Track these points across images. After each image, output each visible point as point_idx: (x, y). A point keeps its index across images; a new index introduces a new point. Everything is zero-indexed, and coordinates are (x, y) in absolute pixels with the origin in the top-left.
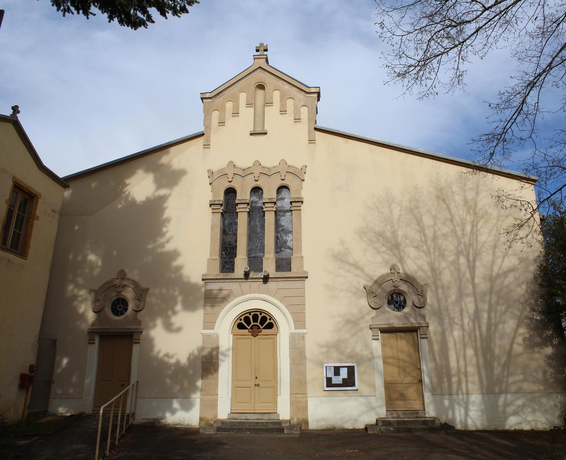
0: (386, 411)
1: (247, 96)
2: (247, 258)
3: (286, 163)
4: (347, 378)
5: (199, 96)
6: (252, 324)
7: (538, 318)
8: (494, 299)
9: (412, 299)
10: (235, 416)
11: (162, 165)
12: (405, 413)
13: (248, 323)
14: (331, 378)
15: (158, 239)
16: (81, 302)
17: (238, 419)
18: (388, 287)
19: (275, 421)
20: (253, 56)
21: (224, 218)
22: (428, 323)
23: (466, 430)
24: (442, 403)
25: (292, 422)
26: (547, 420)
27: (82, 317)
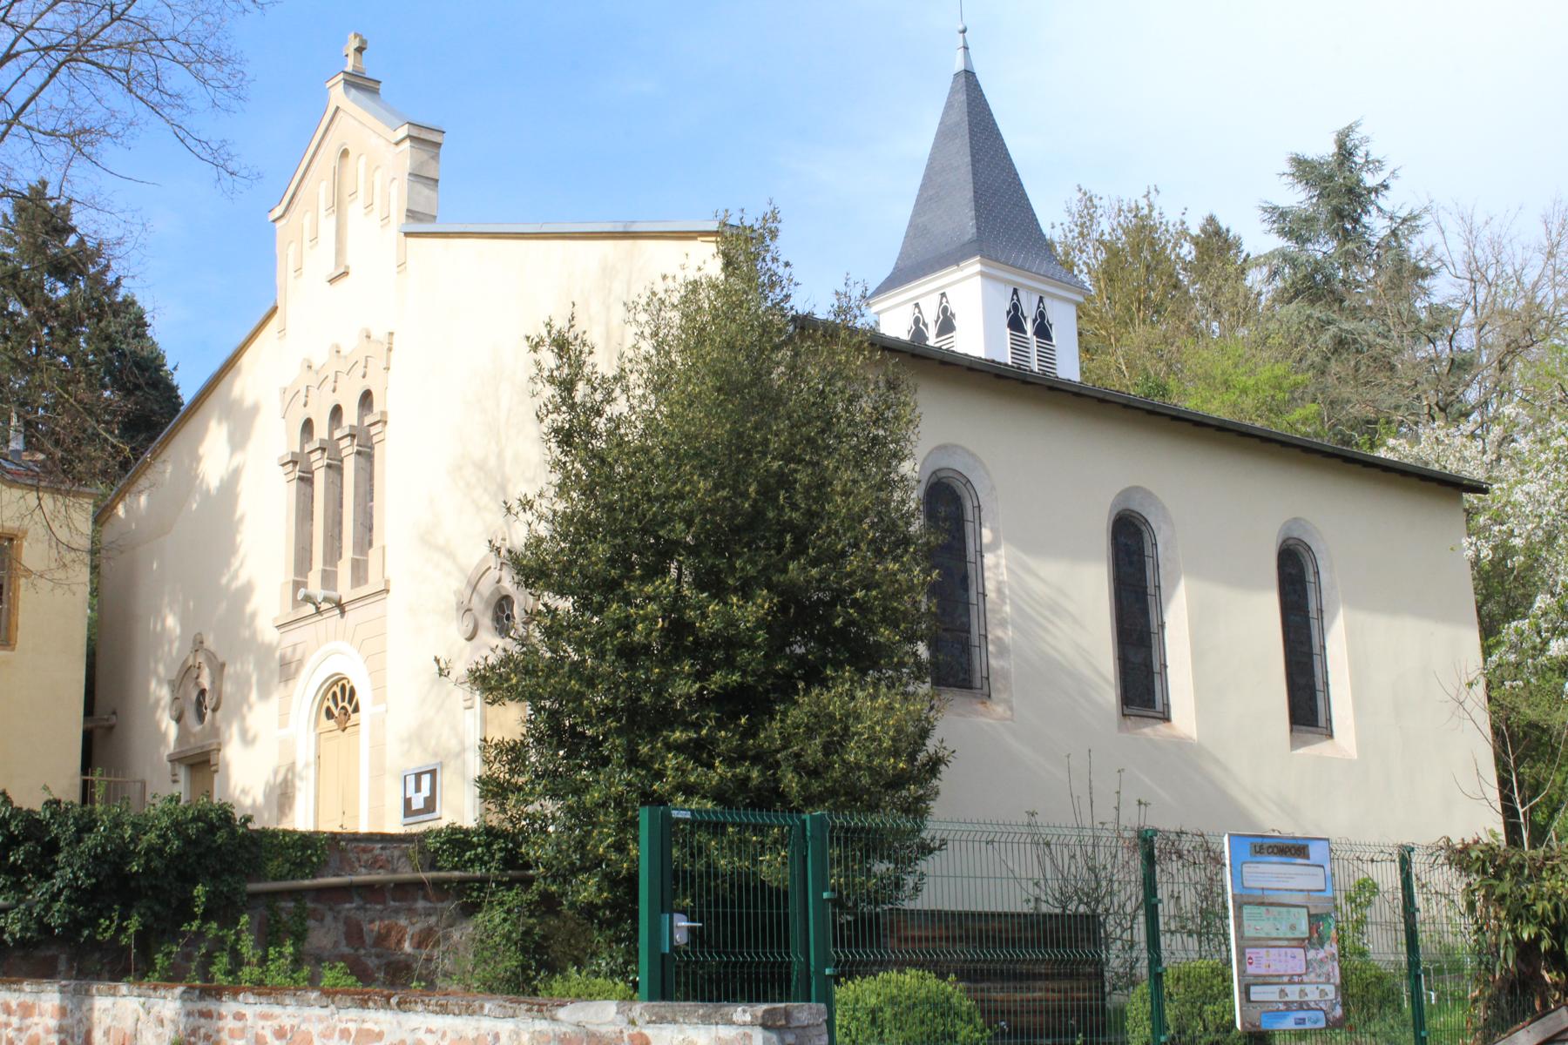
18: (486, 587)
27: (164, 736)
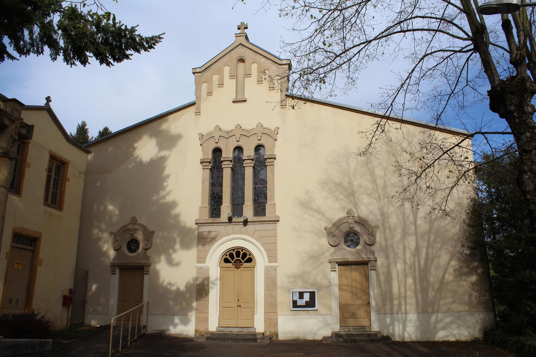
0: (340, 326)
1: (230, 69)
2: (230, 206)
3: (262, 126)
4: (309, 300)
5: (191, 71)
6: (236, 258)
7: (468, 252)
8: (432, 237)
9: (364, 238)
10: (222, 329)
11: (162, 131)
12: (355, 328)
13: (232, 258)
14: (297, 301)
15: (161, 192)
16: (104, 242)
17: (224, 332)
18: (345, 228)
19: (251, 333)
20: (235, 34)
21: (213, 172)
22: (376, 258)
23: (403, 342)
24: (385, 320)
25: (265, 335)
26: (469, 333)
27: (105, 254)
